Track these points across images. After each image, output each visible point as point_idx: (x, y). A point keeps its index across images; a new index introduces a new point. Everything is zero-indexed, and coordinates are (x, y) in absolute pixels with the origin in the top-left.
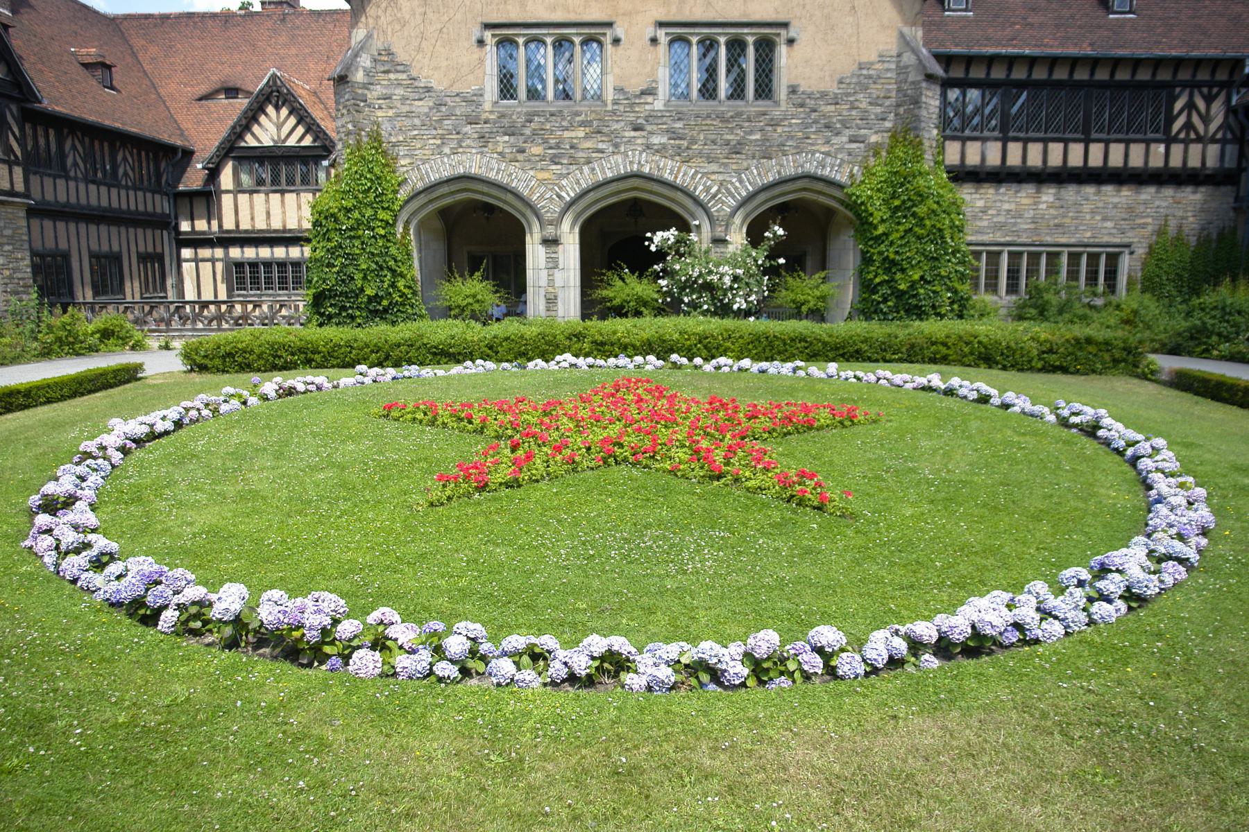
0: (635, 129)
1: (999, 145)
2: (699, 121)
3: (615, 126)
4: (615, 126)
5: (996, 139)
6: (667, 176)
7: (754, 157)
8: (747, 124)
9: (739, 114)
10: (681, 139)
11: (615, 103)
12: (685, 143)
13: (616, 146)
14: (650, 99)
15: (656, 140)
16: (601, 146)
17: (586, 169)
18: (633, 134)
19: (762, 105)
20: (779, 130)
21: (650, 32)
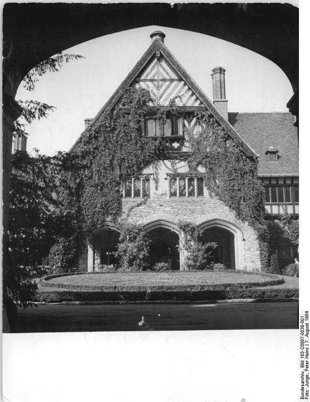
0: (161, 206)
1: (292, 206)
2: (181, 203)
3: (154, 205)
4: (154, 205)
5: (290, 204)
6: (171, 221)
7: (199, 214)
8: (195, 204)
9: (193, 201)
10: (174, 208)
11: (154, 198)
12: (176, 210)
13: (154, 211)
14: (164, 196)
15: (168, 209)
16: (150, 211)
17: (145, 218)
18: (160, 207)
19: (200, 198)
20: (206, 205)
21: (166, 176)
